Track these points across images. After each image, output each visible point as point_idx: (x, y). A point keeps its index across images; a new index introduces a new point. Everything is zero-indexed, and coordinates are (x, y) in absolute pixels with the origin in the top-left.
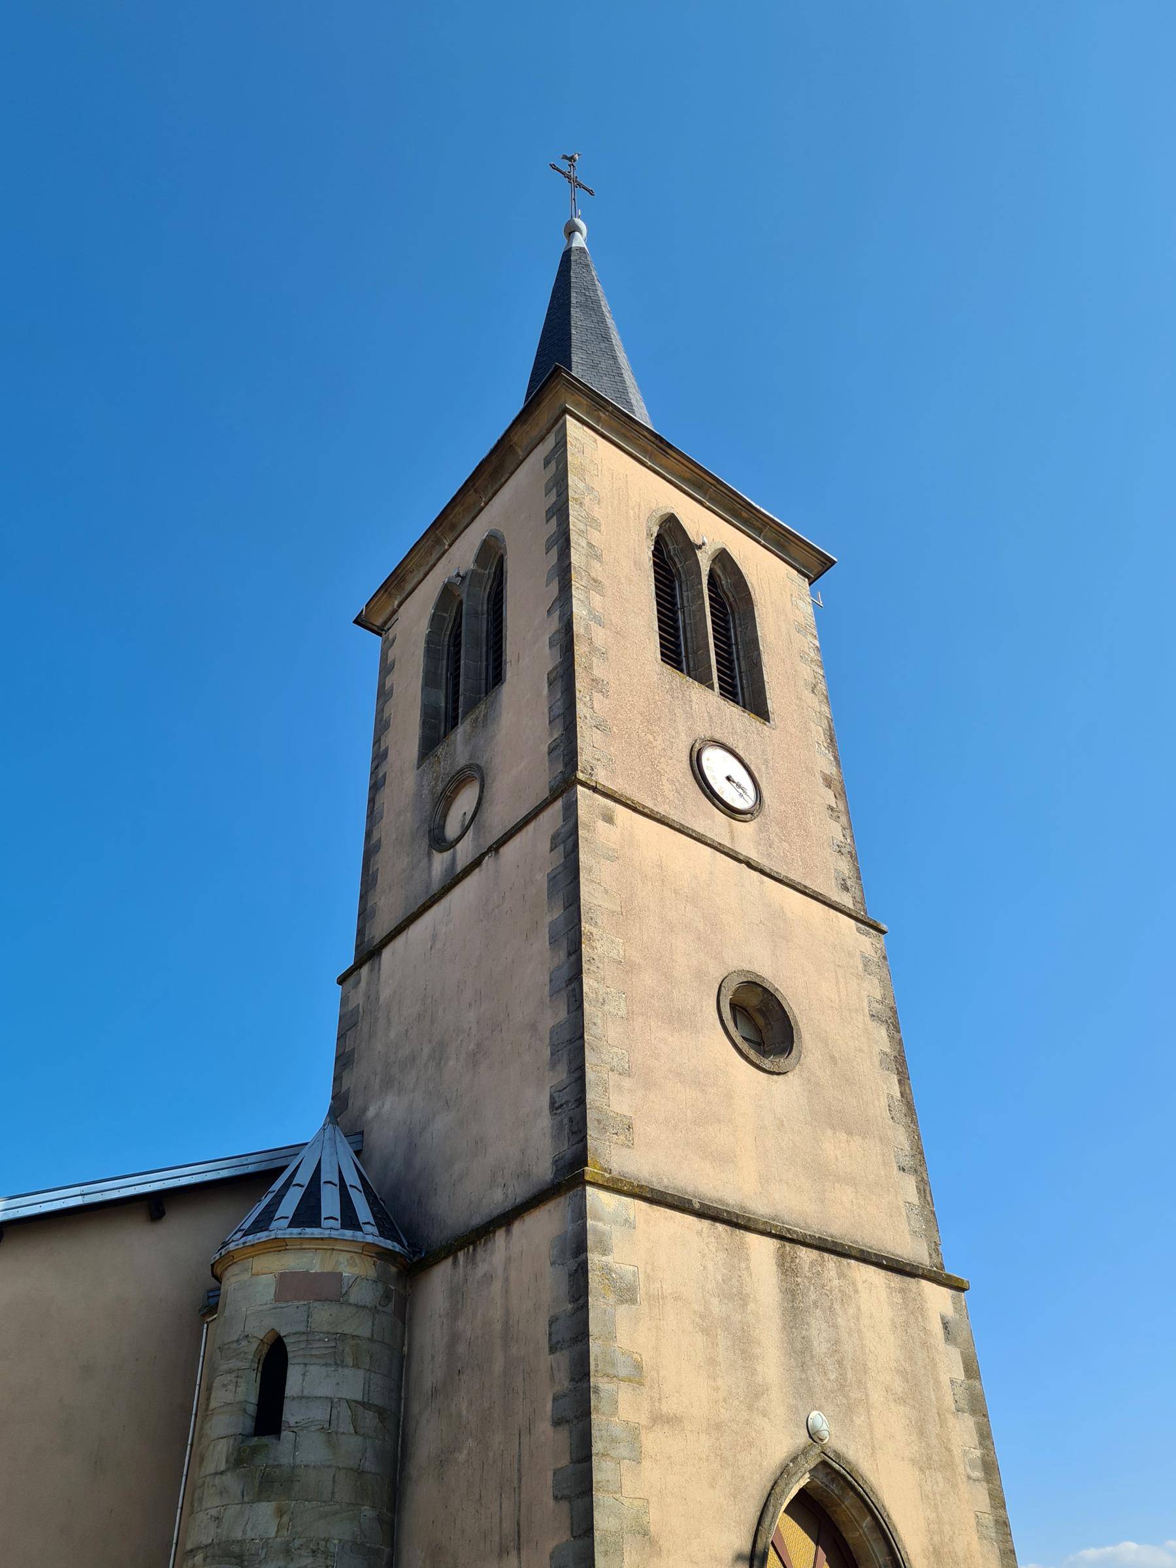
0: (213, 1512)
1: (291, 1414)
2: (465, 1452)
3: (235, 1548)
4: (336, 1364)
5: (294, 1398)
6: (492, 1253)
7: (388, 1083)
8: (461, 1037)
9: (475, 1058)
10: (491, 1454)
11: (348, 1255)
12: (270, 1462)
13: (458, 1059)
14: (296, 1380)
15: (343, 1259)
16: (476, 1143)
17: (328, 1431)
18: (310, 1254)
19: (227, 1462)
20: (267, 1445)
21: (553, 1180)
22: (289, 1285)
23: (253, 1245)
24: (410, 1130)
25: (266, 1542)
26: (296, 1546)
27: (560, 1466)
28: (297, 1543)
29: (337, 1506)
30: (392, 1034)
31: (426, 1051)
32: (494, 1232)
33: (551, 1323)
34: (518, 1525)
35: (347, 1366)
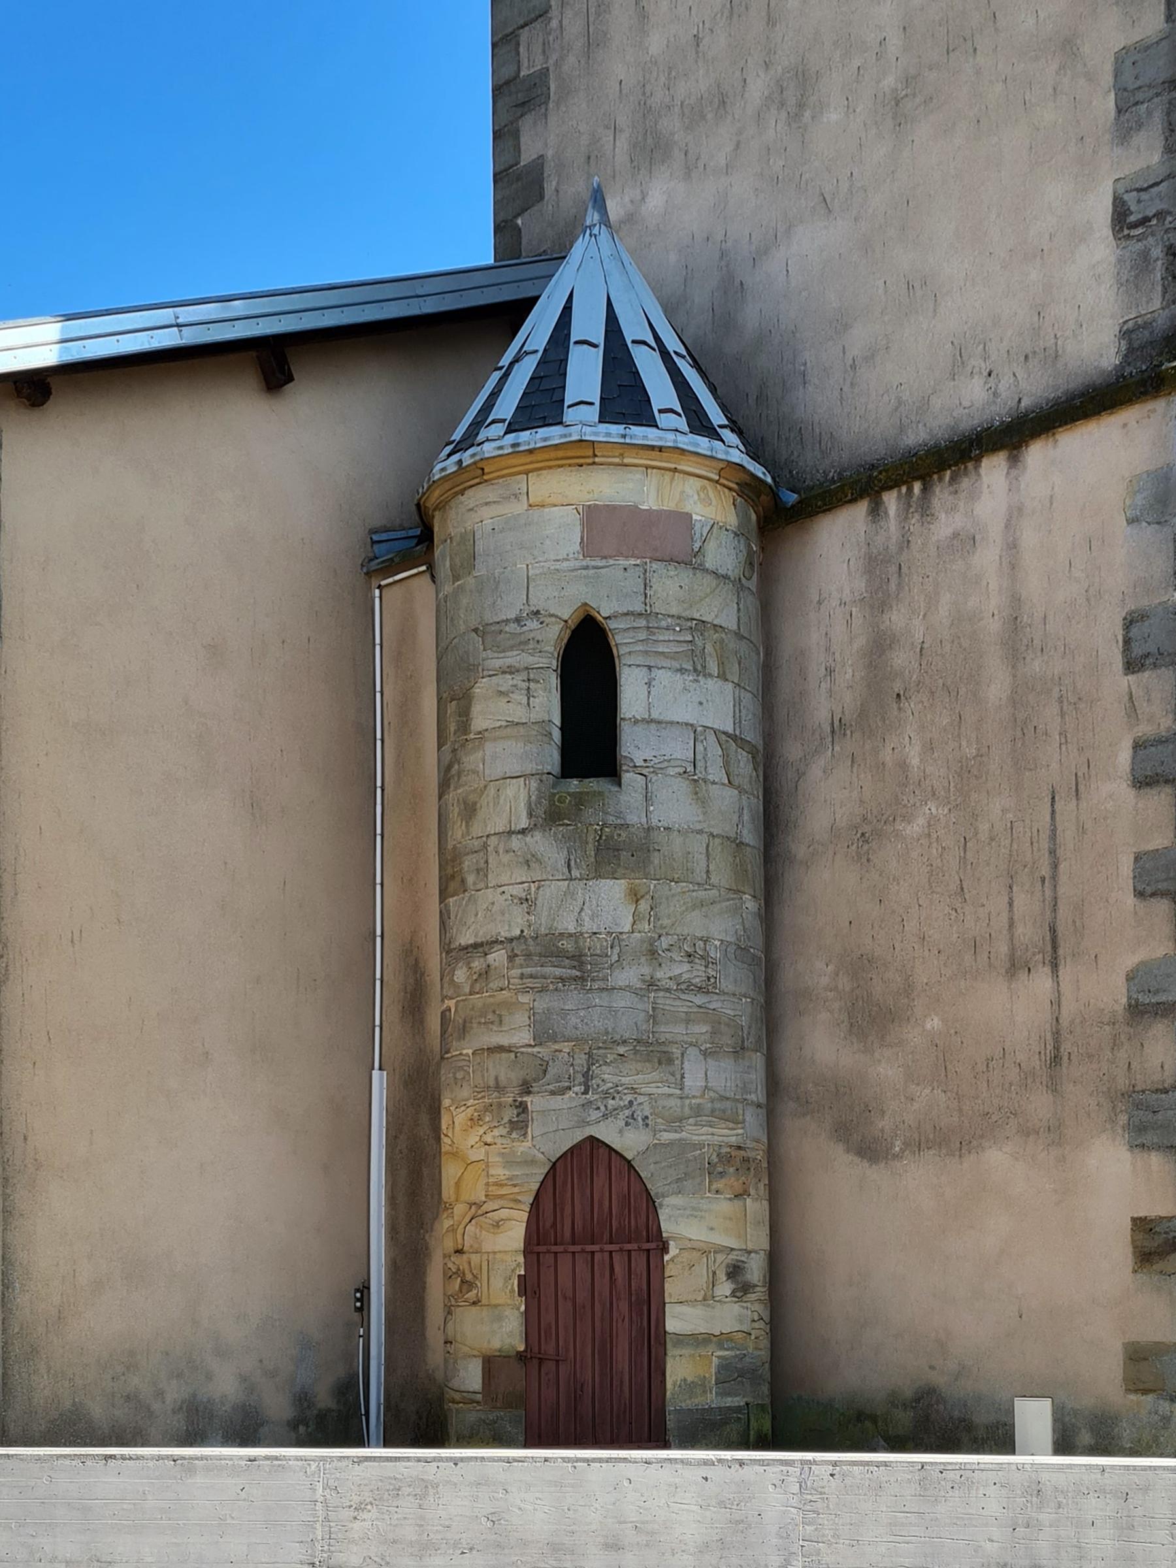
0: (518, 891)
1: (634, 745)
2: (921, 821)
3: (567, 945)
4: (695, 670)
5: (636, 722)
6: (974, 496)
7: (652, 150)
8: (857, 62)
9: (899, 109)
10: (984, 827)
11: (699, 483)
12: (611, 819)
13: (850, 109)
14: (633, 694)
15: (689, 490)
16: (910, 286)
17: (693, 775)
18: (638, 475)
19: (530, 815)
20: (601, 794)
21: (1121, 367)
22: (604, 529)
23: (531, 451)
24: (723, 254)
25: (617, 939)
26: (665, 946)
27: (1150, 847)
28: (665, 942)
29: (715, 892)
30: (656, 43)
31: (758, 87)
32: (978, 460)
33: (1130, 622)
34: (1053, 930)
35: (710, 675)
